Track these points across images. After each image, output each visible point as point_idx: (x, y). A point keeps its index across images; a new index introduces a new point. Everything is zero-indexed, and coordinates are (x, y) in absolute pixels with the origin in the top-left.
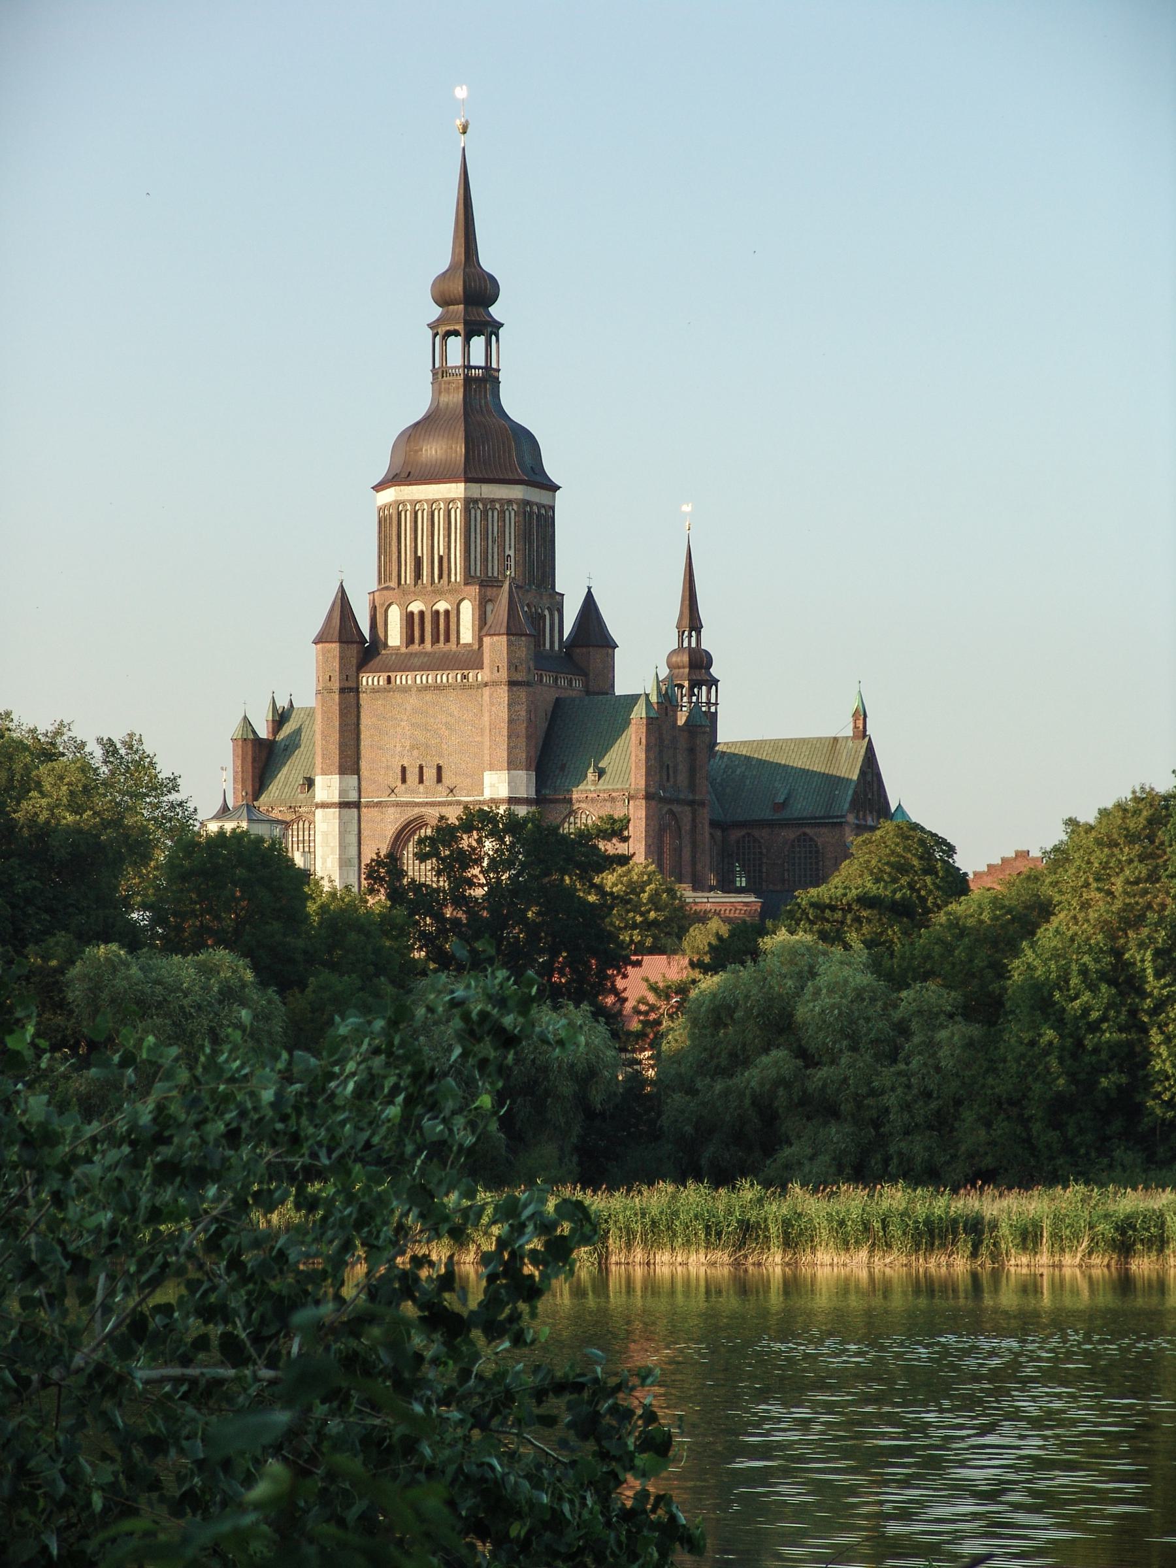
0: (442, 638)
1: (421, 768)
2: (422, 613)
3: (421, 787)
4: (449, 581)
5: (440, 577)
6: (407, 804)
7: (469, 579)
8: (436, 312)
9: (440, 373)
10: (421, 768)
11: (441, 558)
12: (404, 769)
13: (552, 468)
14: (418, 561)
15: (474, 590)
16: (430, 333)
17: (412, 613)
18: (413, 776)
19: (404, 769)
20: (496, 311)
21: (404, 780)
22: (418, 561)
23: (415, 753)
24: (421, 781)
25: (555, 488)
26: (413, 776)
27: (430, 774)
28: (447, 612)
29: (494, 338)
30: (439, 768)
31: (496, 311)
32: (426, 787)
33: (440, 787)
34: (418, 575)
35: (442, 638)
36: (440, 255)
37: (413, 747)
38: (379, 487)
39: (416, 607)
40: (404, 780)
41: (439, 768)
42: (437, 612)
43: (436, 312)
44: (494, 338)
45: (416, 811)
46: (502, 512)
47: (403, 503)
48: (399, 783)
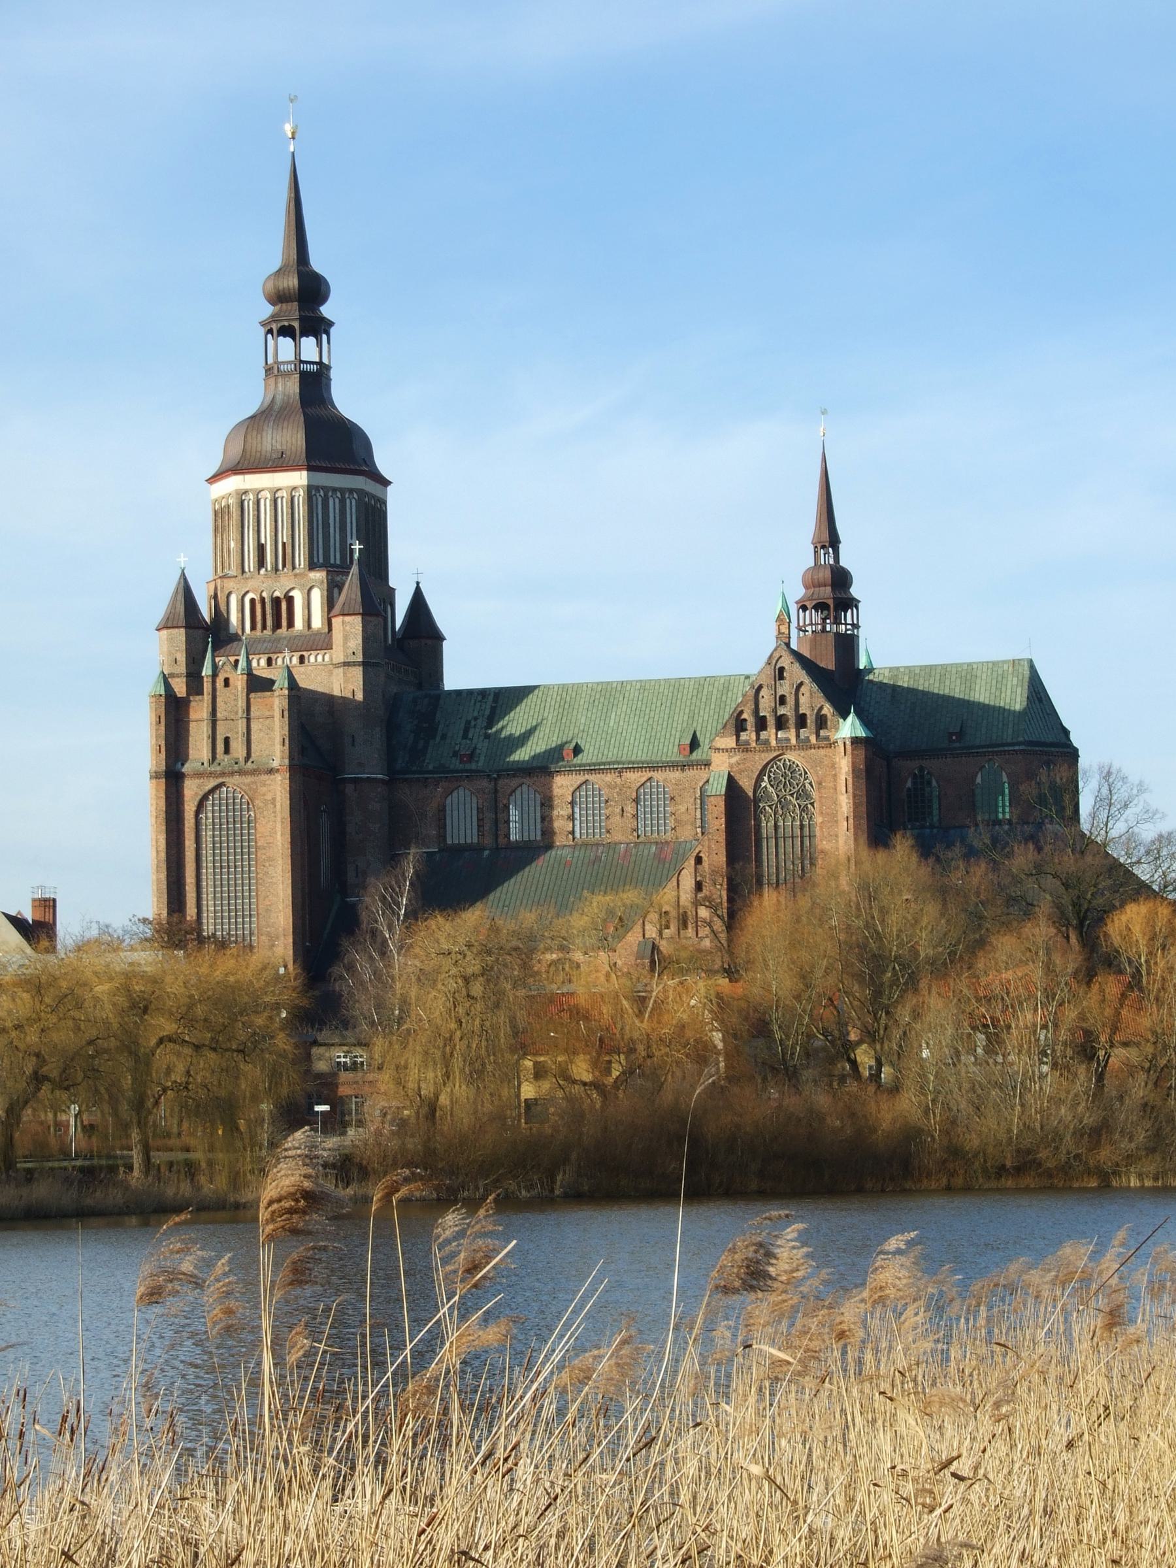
4: (294, 568)
5: (284, 566)
7: (312, 566)
8: (268, 310)
9: (272, 371)
11: (284, 544)
13: (383, 462)
14: (261, 548)
15: (319, 575)
16: (262, 331)
20: (326, 310)
22: (261, 548)
25: (386, 483)
29: (324, 337)
31: (326, 310)
34: (261, 563)
36: (272, 254)
38: (213, 479)
43: (268, 310)
44: (324, 337)
46: (343, 502)
47: (246, 492)
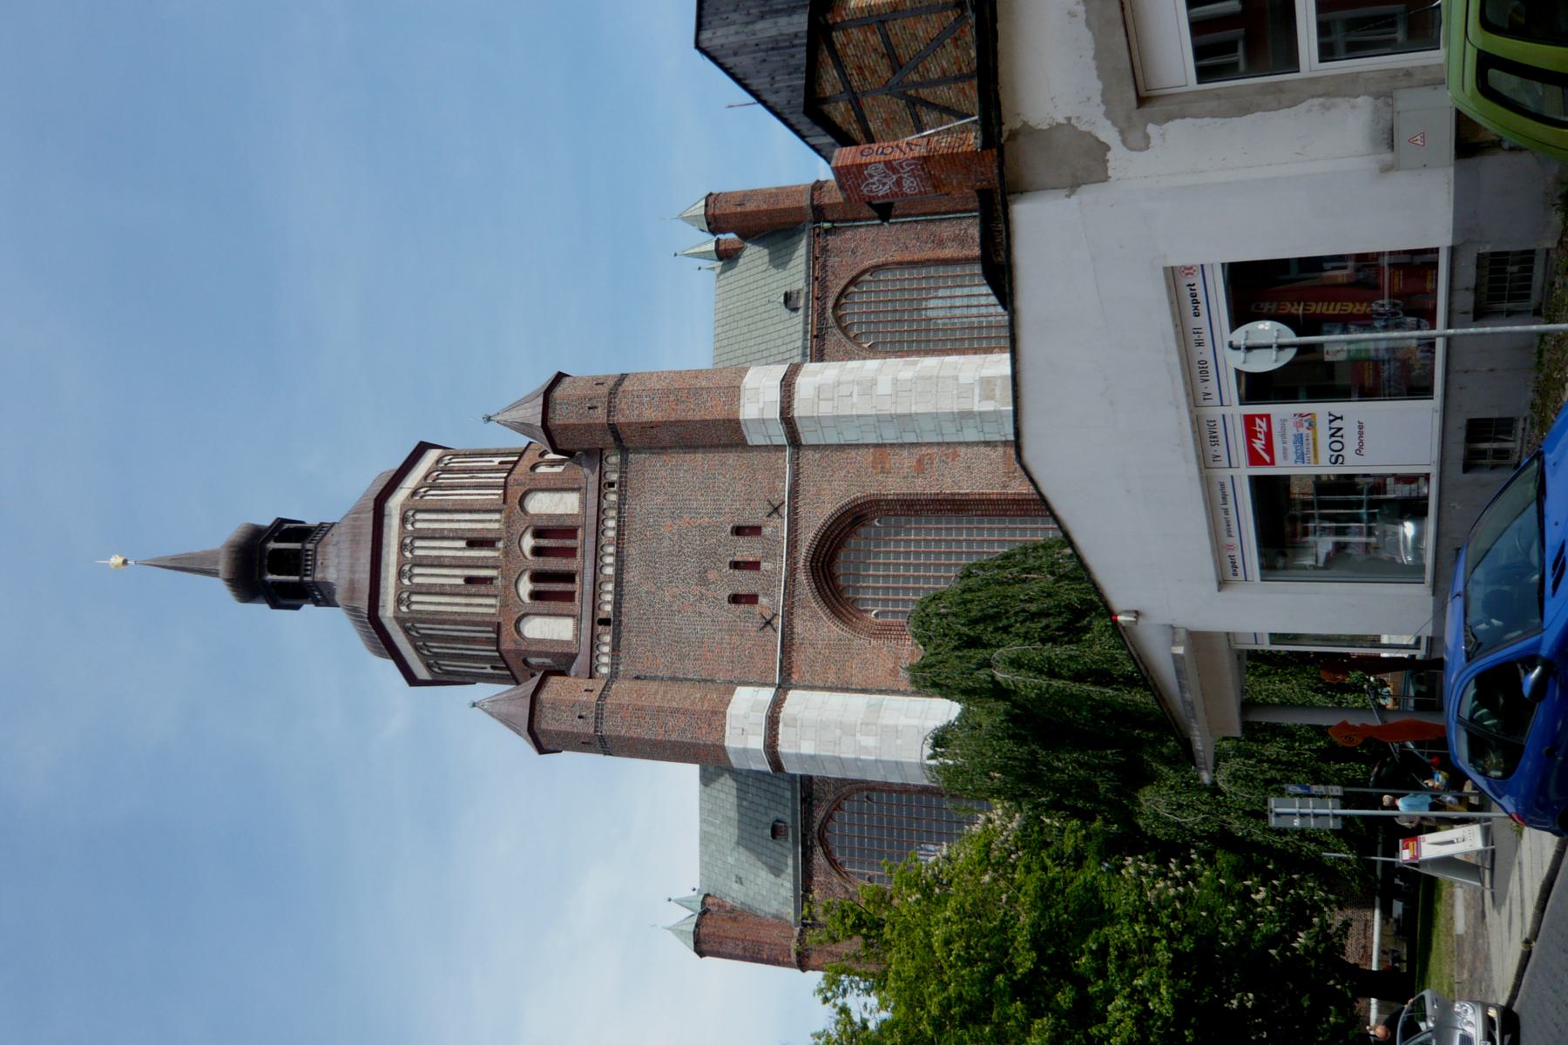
0: (568, 543)
1: (736, 565)
2: (537, 577)
3: (765, 566)
6: (790, 594)
10: (736, 565)
11: (473, 543)
12: (735, 599)
14: (470, 580)
17: (535, 595)
18: (744, 582)
19: (735, 599)
21: (752, 599)
23: (712, 575)
24: (754, 566)
26: (744, 582)
27: (746, 549)
28: (539, 533)
30: (738, 531)
32: (766, 557)
33: (766, 531)
35: (568, 543)
37: (703, 581)
39: (526, 587)
40: (752, 599)
41: (738, 531)
42: (537, 551)
45: (802, 577)
48: (757, 609)
